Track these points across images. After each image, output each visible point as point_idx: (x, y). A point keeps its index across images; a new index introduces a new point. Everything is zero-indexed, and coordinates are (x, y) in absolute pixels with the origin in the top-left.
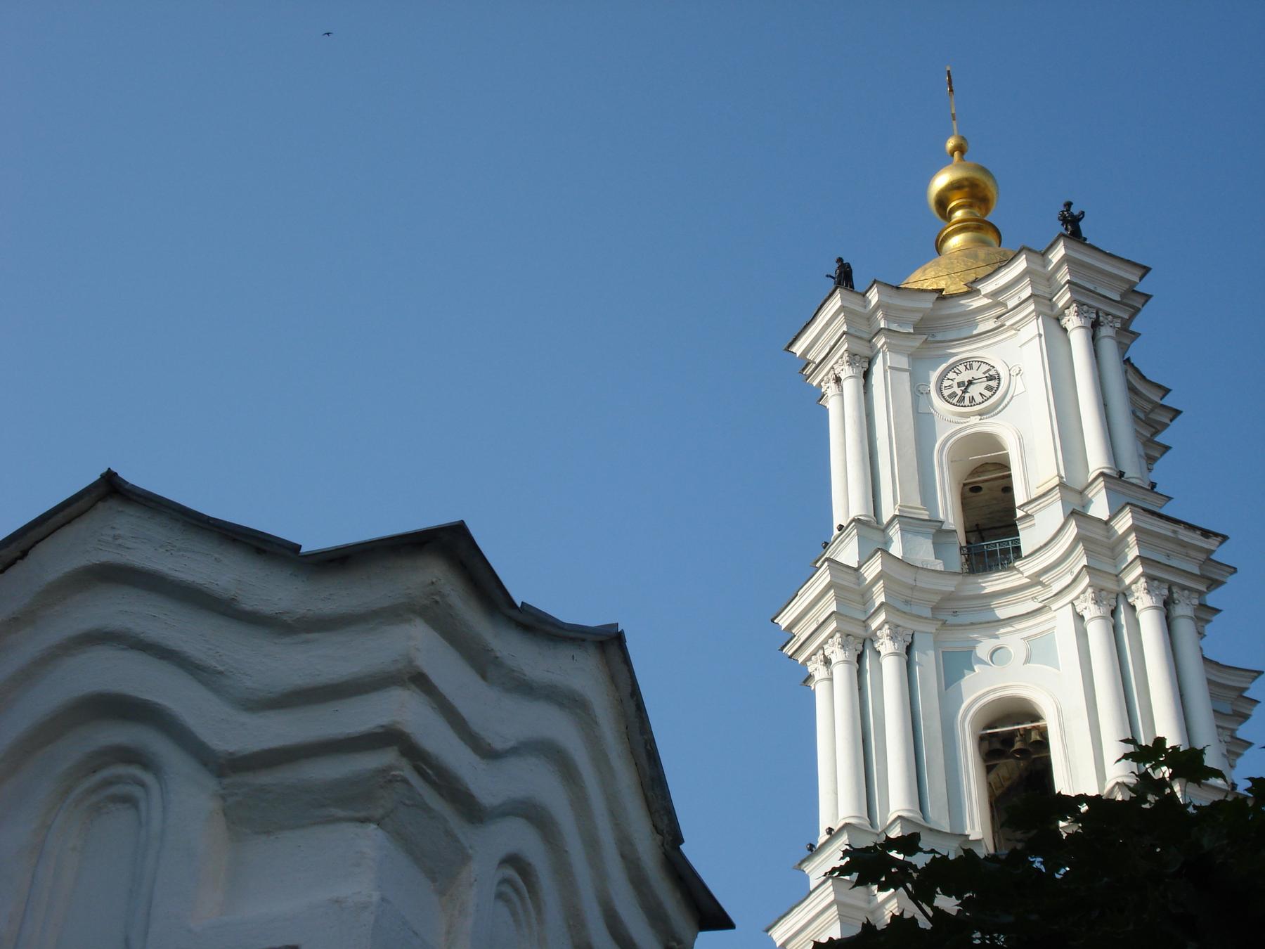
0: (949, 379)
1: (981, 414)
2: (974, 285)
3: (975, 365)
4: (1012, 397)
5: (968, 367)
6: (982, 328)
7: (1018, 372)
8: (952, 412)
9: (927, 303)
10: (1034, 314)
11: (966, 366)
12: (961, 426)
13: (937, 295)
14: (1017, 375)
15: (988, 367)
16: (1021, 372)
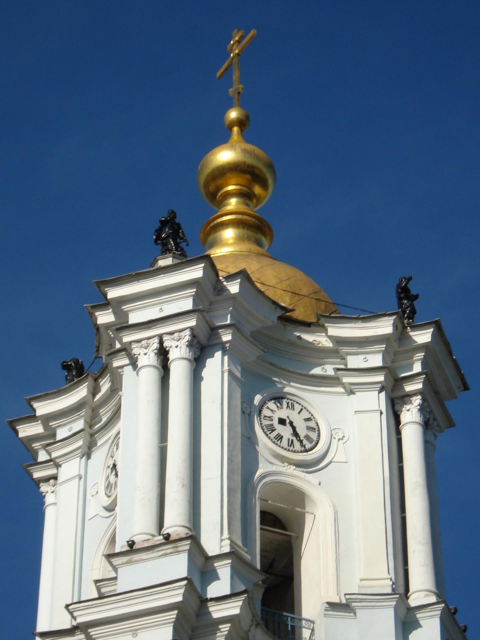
0: (268, 408)
1: (299, 465)
2: (322, 320)
3: (298, 408)
4: (330, 462)
5: (290, 405)
6: (317, 371)
7: (341, 437)
8: (270, 449)
9: (274, 315)
10: (379, 385)
11: (288, 403)
12: (274, 468)
13: (280, 313)
14: (339, 439)
15: (309, 416)
16: (345, 440)
